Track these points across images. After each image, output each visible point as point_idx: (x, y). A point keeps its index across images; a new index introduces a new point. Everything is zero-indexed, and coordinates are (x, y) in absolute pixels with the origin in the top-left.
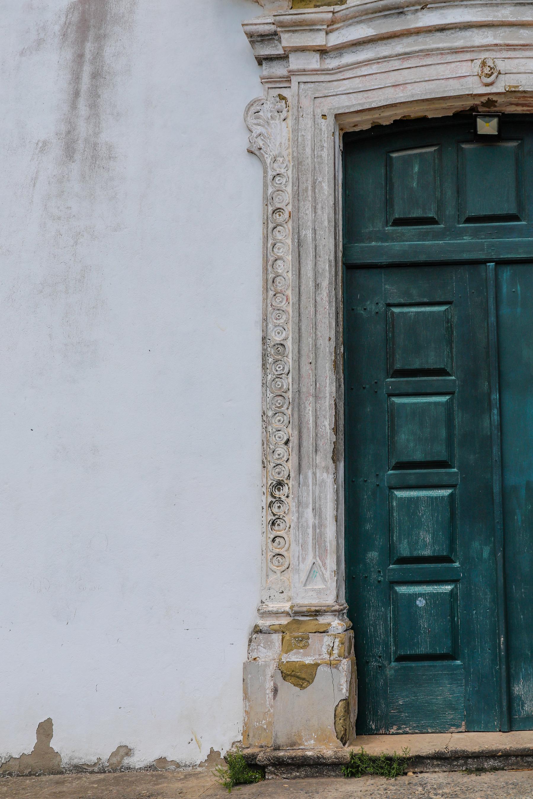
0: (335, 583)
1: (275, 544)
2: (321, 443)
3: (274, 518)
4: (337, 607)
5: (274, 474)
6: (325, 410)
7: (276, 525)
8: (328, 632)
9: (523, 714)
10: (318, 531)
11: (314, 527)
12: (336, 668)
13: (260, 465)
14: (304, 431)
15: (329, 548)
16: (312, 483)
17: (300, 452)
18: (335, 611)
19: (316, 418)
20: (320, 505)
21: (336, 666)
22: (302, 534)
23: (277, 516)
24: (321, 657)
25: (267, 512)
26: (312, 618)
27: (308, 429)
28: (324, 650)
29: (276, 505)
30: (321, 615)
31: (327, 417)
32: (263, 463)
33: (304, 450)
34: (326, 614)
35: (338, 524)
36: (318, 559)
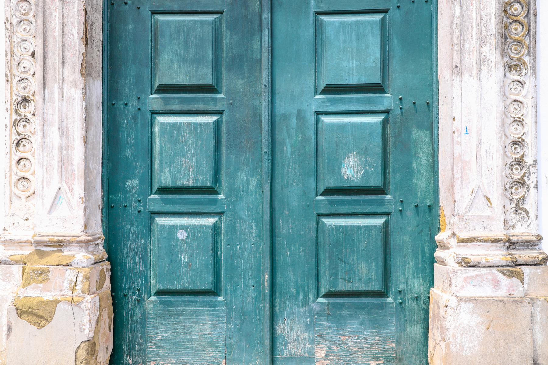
0: (83, 211)
1: (20, 166)
2: (68, 54)
3: (19, 138)
4: (83, 238)
5: (19, 88)
6: (73, 17)
7: (21, 145)
8: (71, 265)
9: (286, 354)
10: (64, 152)
11: (61, 149)
12: (77, 305)
13: (4, 79)
14: (50, 40)
15: (76, 173)
16: (59, 99)
17: (44, 63)
18: (81, 242)
19: (63, 25)
20: (67, 124)
21: (78, 305)
22: (47, 156)
23: (22, 136)
24: (63, 293)
25: (11, 131)
26: (56, 249)
27: (54, 38)
28: (66, 285)
29: (22, 123)
30: (67, 246)
31: (76, 24)
32: (6, 76)
33: (49, 62)
34: (71, 244)
35: (89, 146)
36: (64, 183)
